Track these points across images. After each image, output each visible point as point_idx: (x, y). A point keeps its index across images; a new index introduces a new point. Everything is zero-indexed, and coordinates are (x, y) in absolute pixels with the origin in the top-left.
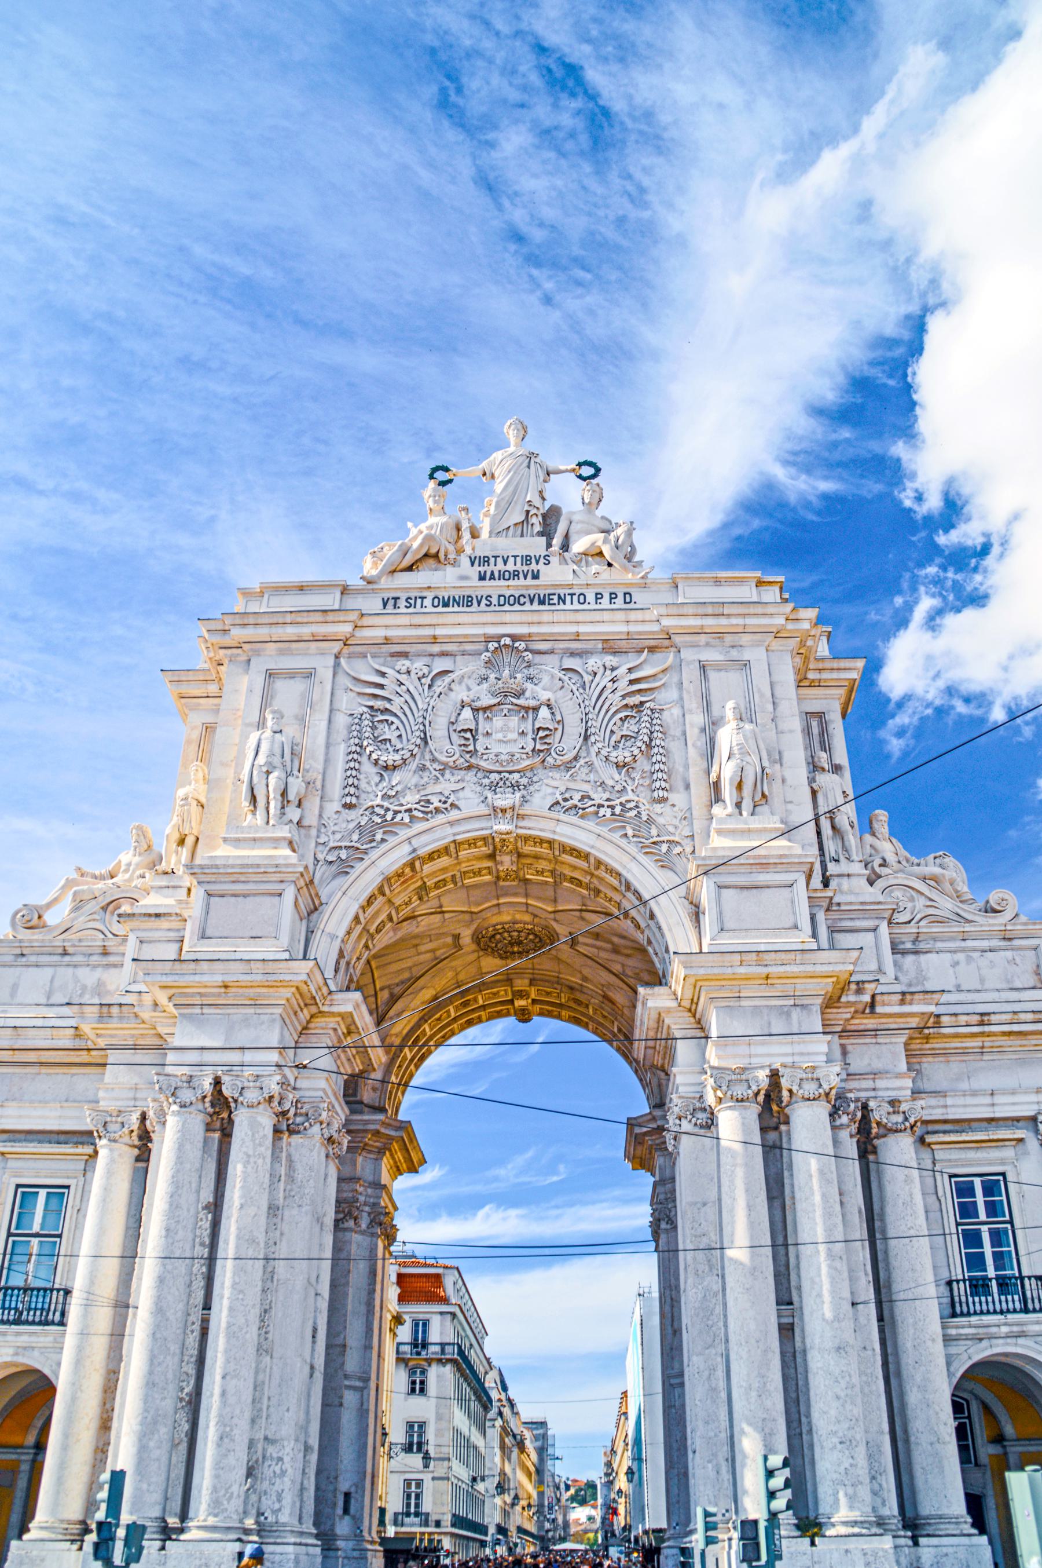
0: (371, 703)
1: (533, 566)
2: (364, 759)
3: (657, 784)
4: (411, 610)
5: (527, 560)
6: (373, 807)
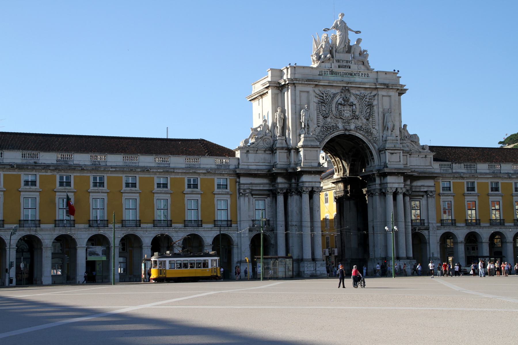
0: (321, 101)
1: (349, 64)
2: (320, 114)
3: (374, 124)
4: (325, 75)
5: (347, 62)
6: (323, 127)
